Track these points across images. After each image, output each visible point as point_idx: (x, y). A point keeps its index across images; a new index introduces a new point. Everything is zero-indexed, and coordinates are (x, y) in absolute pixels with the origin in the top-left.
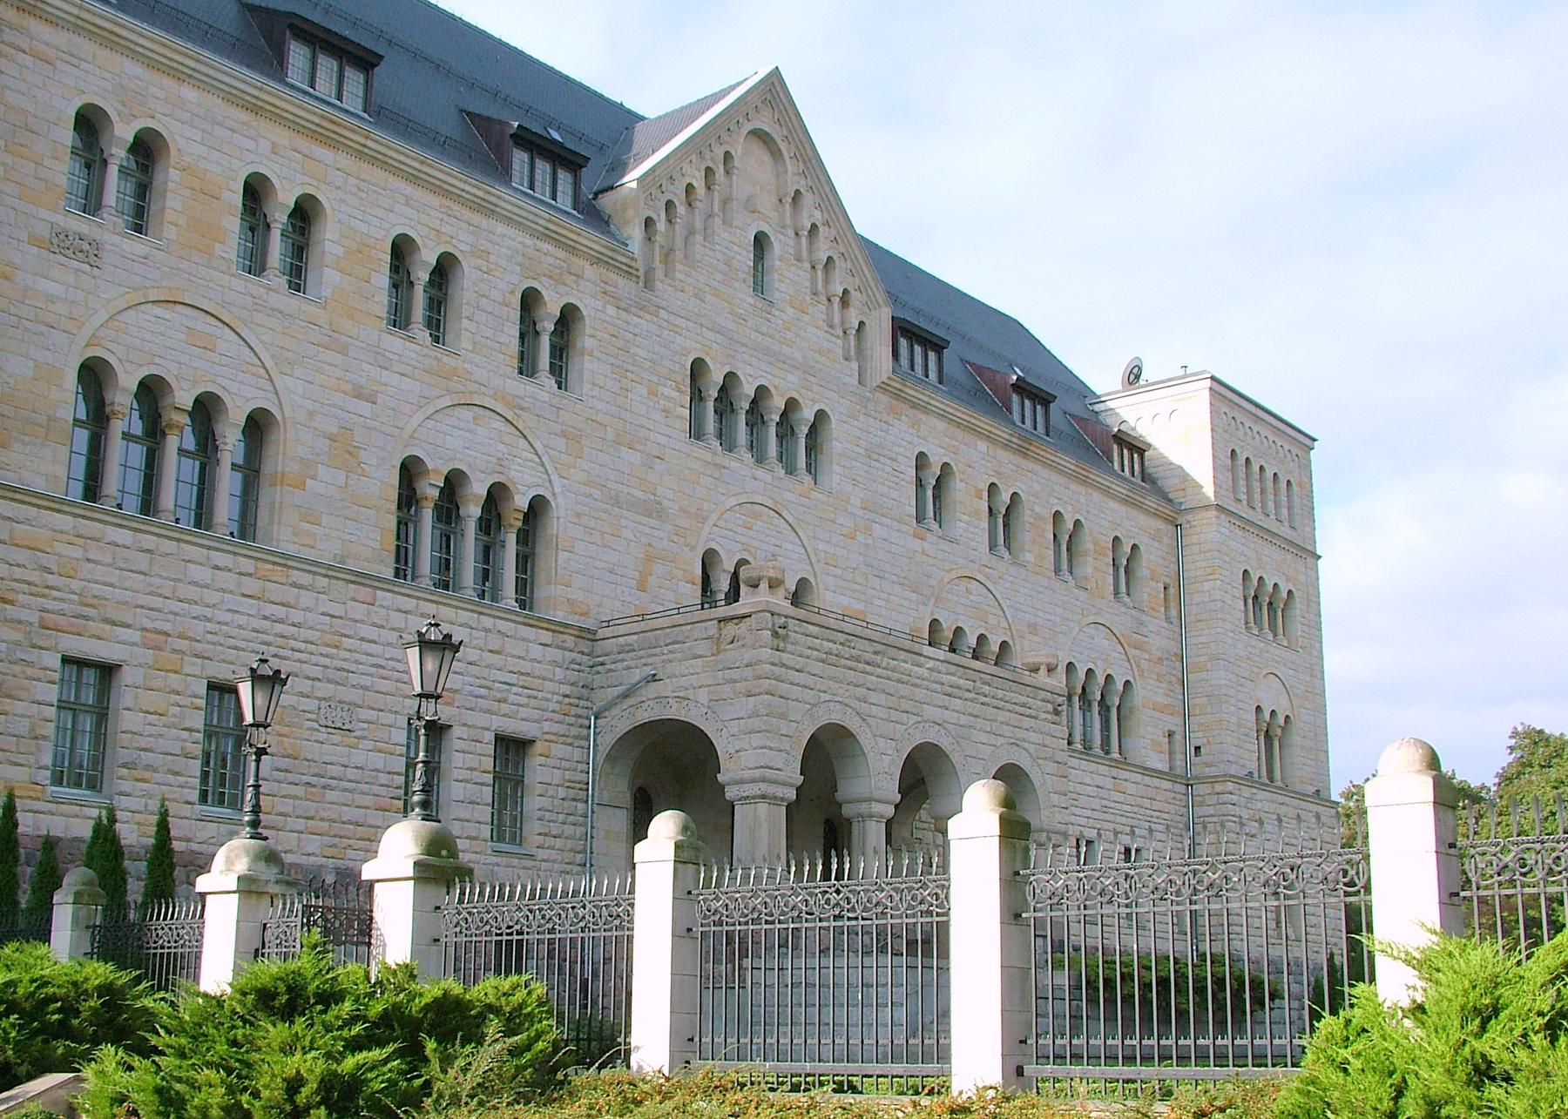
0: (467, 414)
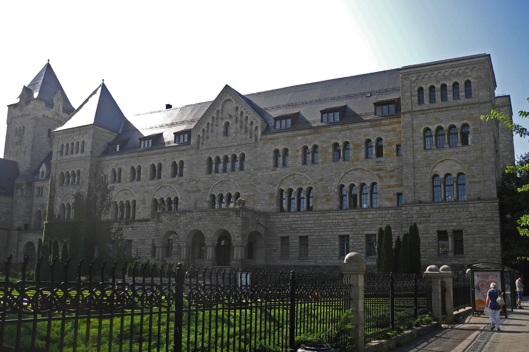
0: (163, 188)
